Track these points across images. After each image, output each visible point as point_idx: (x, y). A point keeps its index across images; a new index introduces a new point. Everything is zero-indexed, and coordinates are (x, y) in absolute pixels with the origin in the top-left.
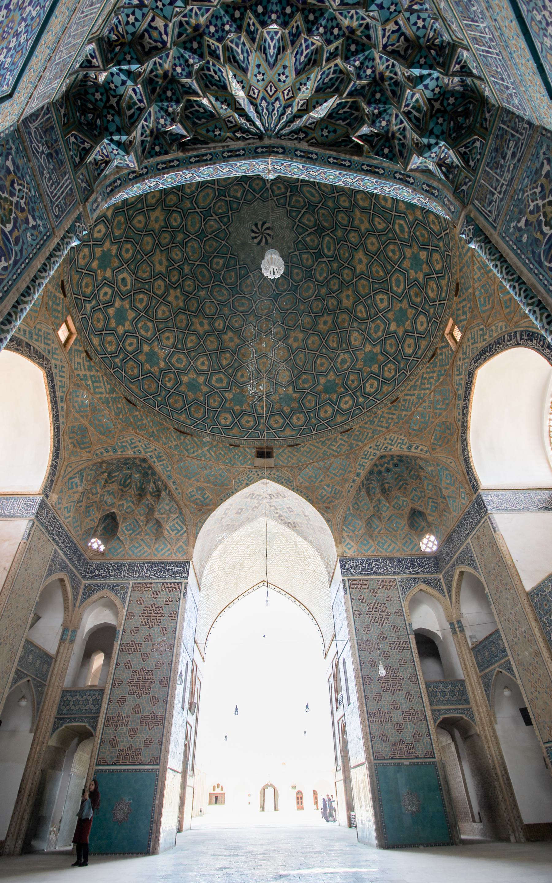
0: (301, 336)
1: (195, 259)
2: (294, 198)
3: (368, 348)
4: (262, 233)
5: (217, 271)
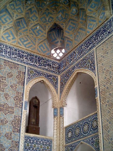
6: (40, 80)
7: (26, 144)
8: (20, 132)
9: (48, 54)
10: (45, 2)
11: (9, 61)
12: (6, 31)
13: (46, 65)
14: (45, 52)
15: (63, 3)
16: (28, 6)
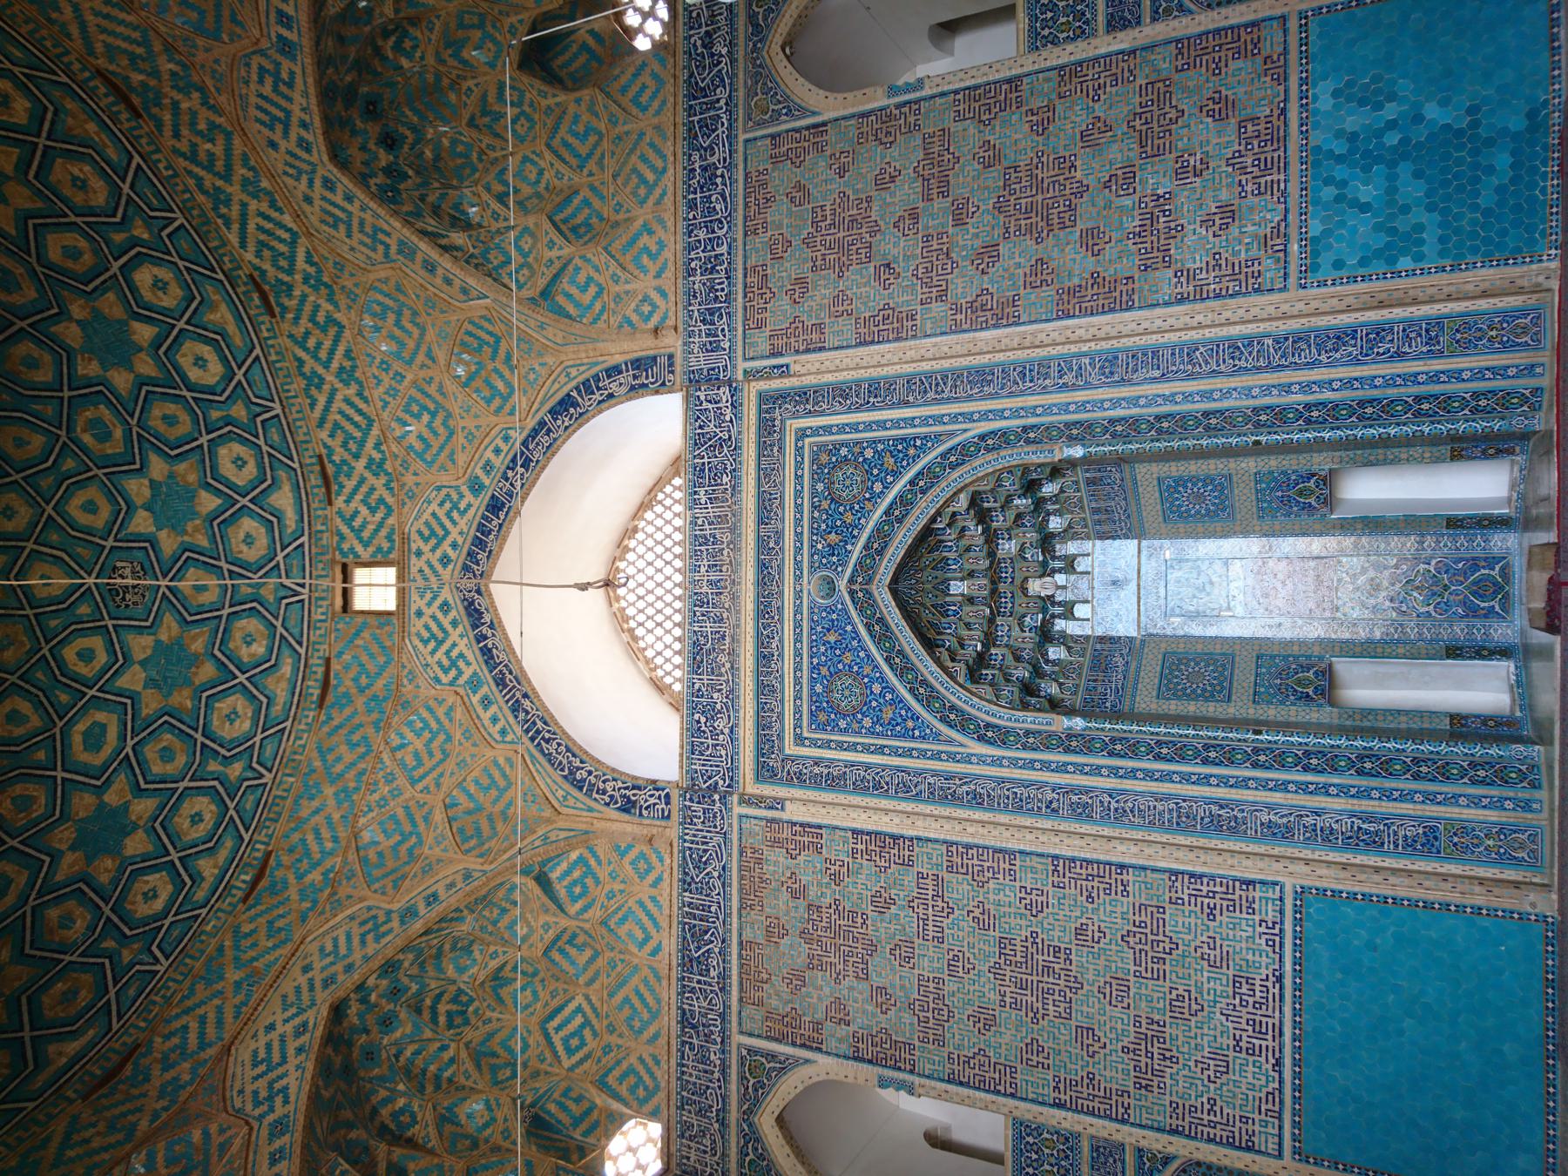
6: (785, 62)
7: (1062, 36)
8: (1019, 78)
9: (663, 63)
10: (446, 142)
11: (745, 218)
12: (631, 267)
13: (713, 55)
14: (655, 76)
15: (418, 54)
16: (489, 212)
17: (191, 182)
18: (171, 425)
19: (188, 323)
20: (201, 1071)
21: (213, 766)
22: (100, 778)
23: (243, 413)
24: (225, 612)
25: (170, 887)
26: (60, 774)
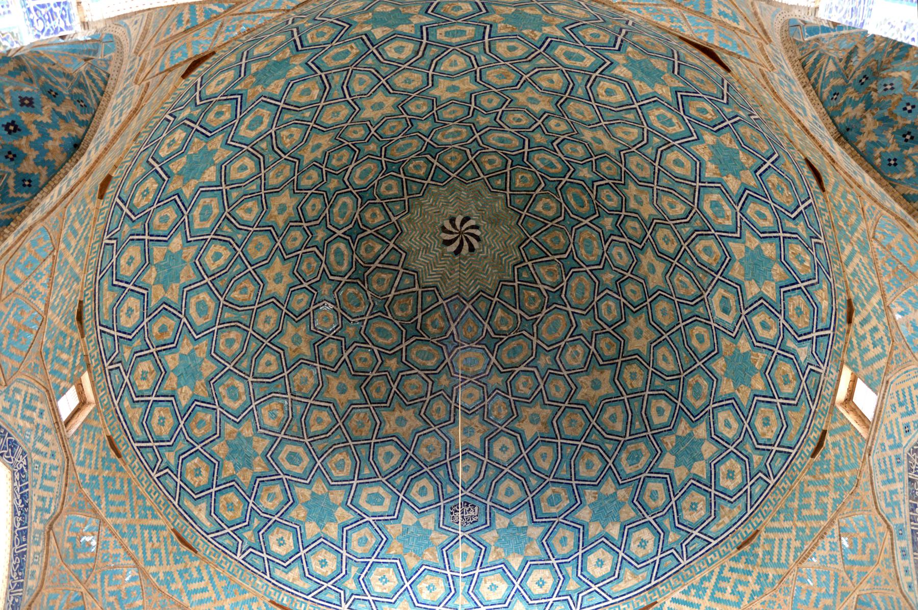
0: (367, 113)
1: (589, 231)
2: (410, 311)
3: (210, 175)
4: (460, 233)
5: (550, 197)
17: (706, 573)
18: (561, 542)
19: (623, 558)
20: (175, 597)
21: (354, 570)
22: (351, 504)
23: (572, 588)
24: (448, 572)
25: (284, 553)
26: (355, 482)
